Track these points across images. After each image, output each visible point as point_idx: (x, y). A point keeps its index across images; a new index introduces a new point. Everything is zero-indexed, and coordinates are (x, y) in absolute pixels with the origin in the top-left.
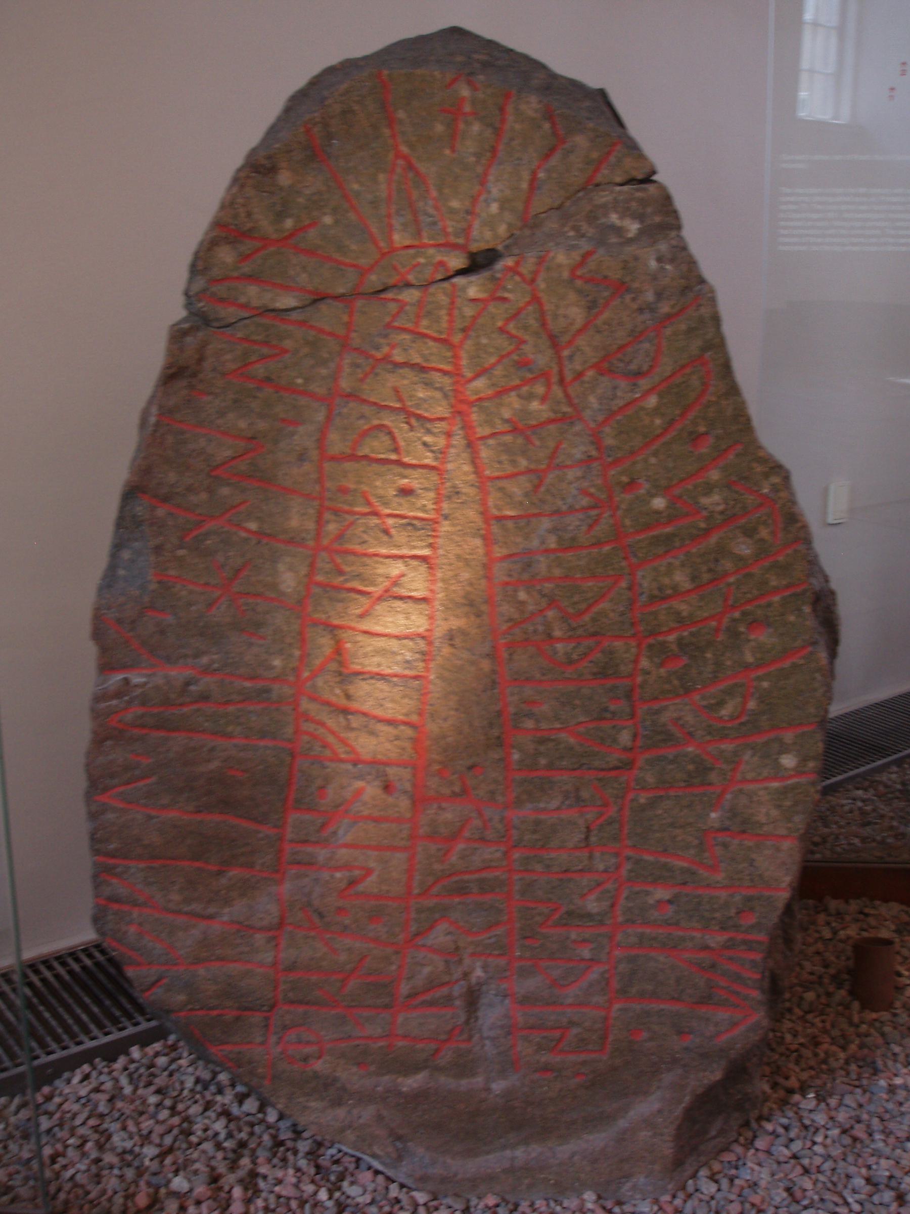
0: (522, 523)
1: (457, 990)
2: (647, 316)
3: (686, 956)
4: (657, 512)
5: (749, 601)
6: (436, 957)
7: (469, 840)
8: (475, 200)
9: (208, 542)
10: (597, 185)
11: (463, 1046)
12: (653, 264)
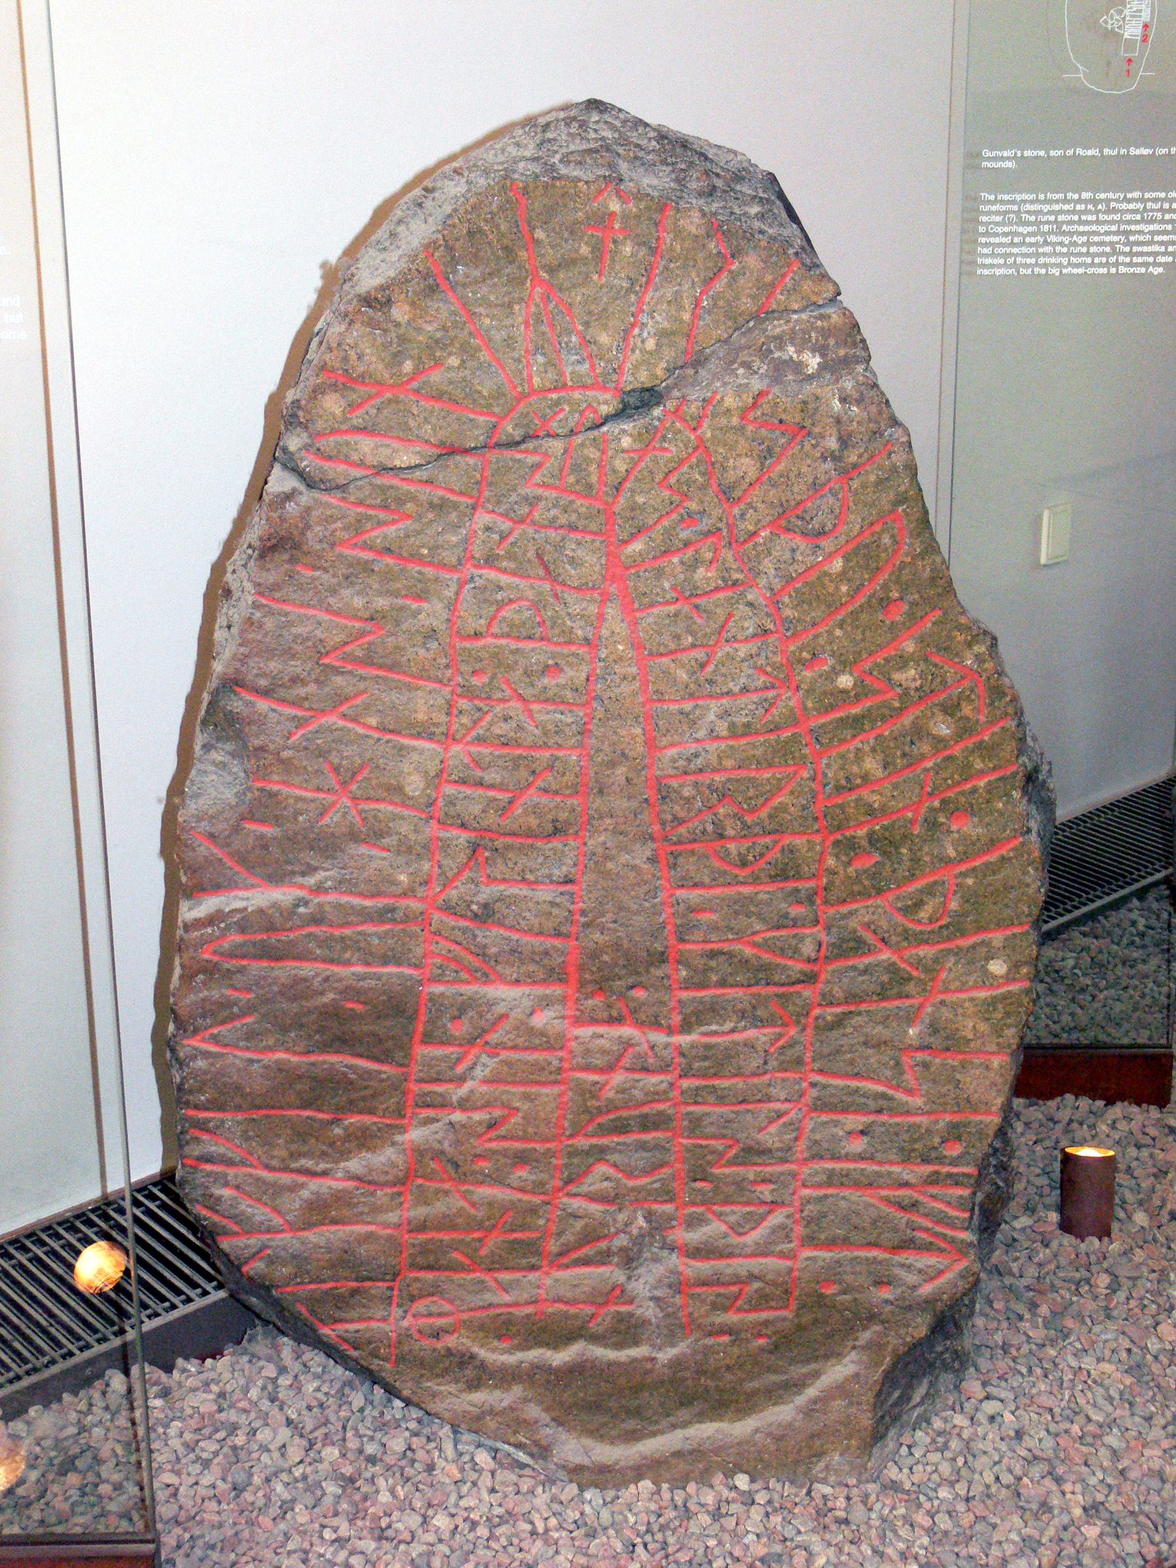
0: (688, 706)
2: (829, 465)
3: (884, 1193)
4: (844, 691)
5: (949, 787)
7: (627, 1070)
8: (627, 333)
12: (836, 405)
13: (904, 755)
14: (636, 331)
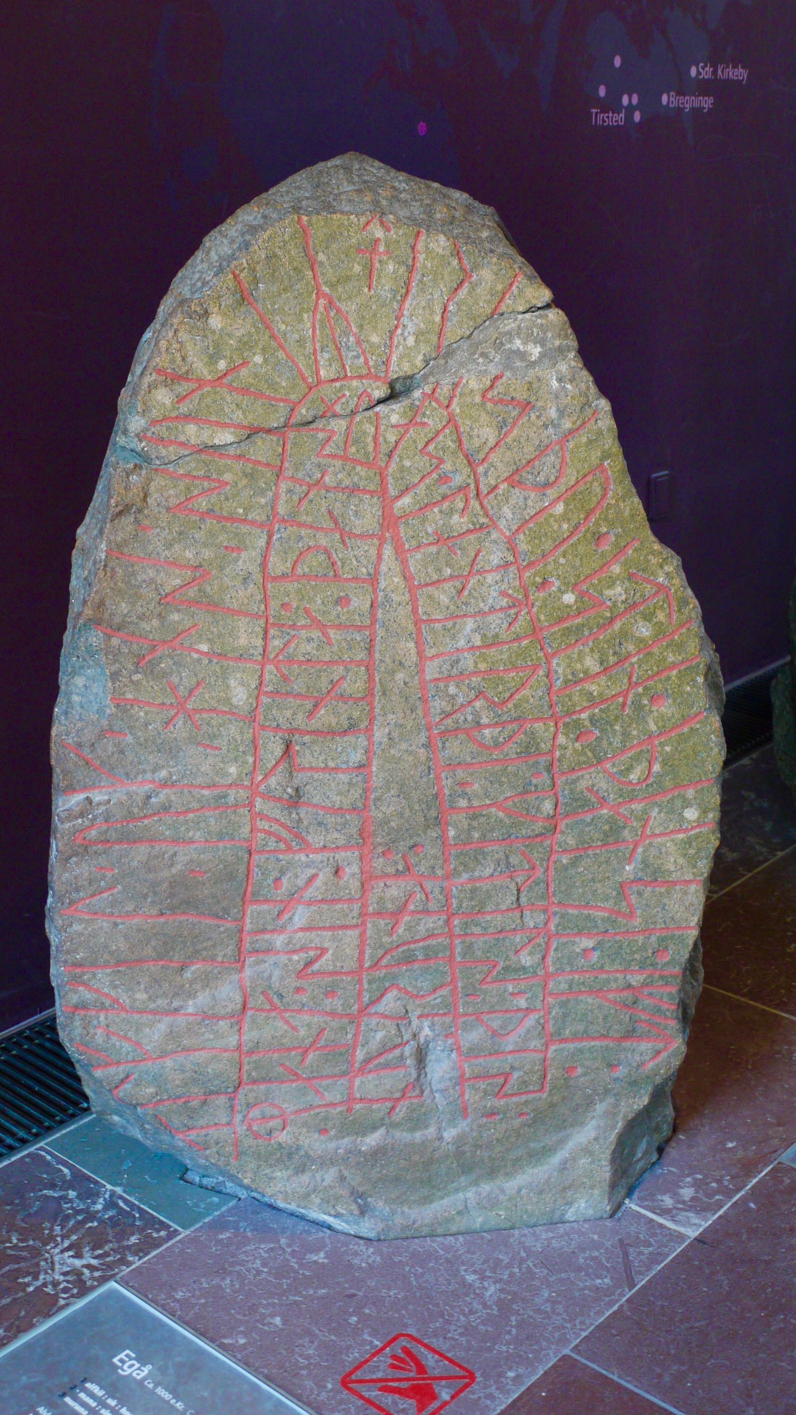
0: (449, 624)
1: (408, 1050)
4: (568, 606)
5: (650, 678)
6: (388, 1022)
8: (392, 333)
9: (163, 665)
10: (502, 314)
11: (416, 1101)
12: (555, 384)
13: (615, 653)
14: (399, 331)
